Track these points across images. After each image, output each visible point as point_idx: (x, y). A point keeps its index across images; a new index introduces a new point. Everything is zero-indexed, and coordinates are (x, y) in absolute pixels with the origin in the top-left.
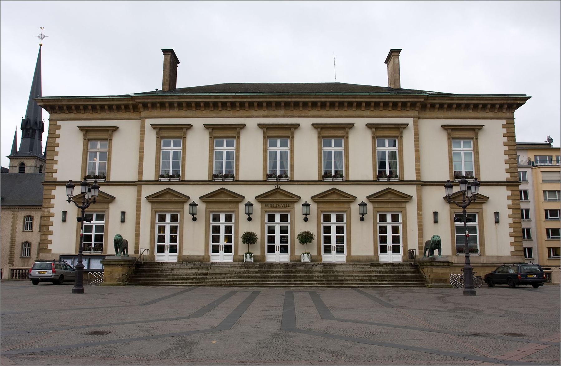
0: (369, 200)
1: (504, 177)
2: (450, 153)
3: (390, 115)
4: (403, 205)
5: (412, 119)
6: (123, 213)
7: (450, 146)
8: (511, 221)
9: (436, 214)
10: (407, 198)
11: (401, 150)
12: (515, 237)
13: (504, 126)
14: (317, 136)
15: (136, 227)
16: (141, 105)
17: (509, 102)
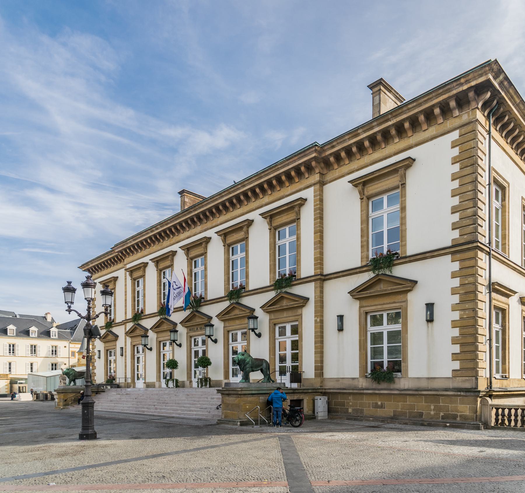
4: (299, 311)
8: (456, 316)
9: (341, 318)
12: (462, 345)
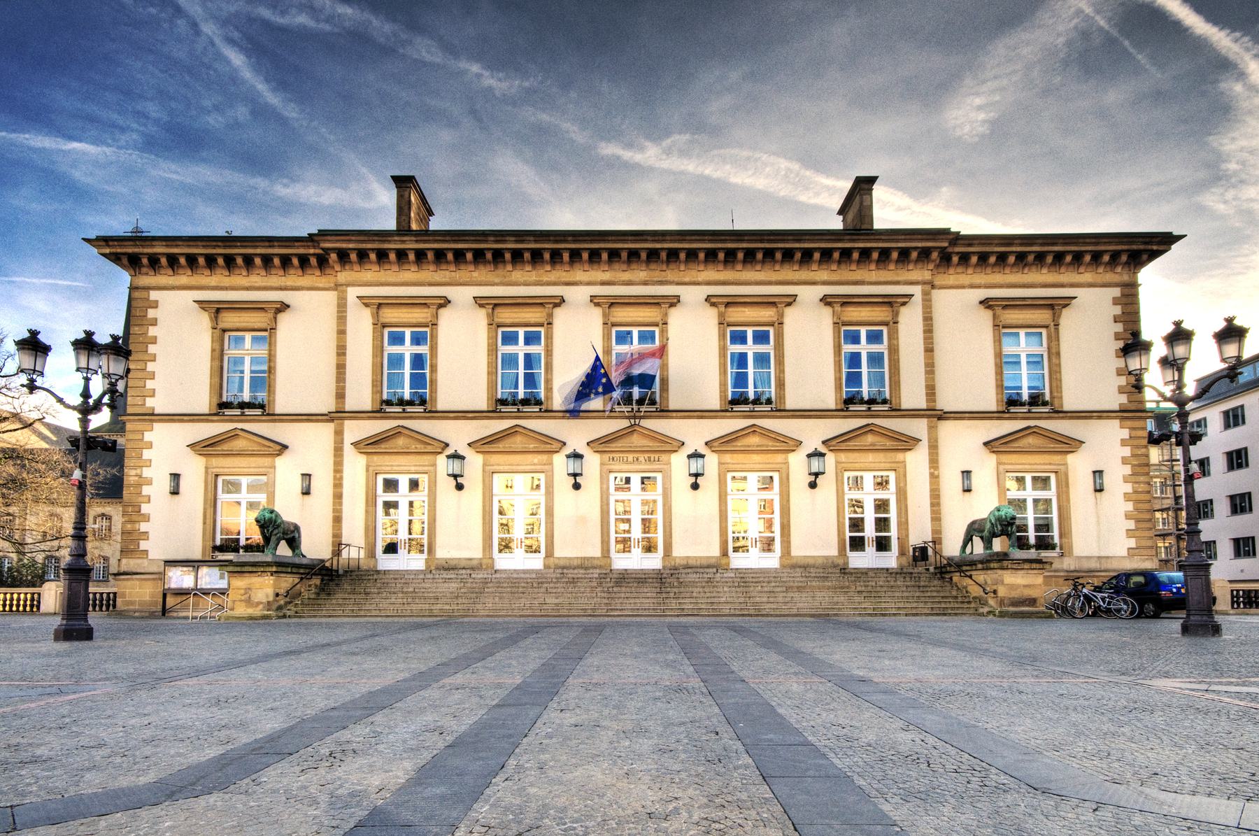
0: (828, 447)
1: (1115, 400)
2: (999, 355)
3: (874, 279)
6: (307, 476)
7: (998, 342)
8: (1128, 488)
11: (894, 350)
14: (716, 322)
15: (334, 504)
16: (334, 256)
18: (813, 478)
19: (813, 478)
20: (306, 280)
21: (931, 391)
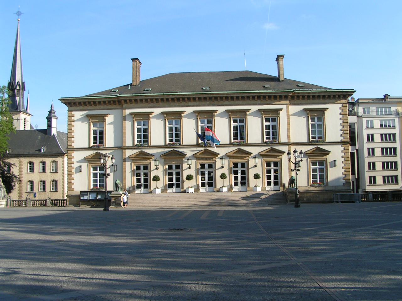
5: (286, 105)
10: (283, 152)
13: (340, 108)
16: (123, 101)
17: (344, 94)
18: (255, 164)
19: (255, 164)
20: (114, 106)
21: (289, 137)
